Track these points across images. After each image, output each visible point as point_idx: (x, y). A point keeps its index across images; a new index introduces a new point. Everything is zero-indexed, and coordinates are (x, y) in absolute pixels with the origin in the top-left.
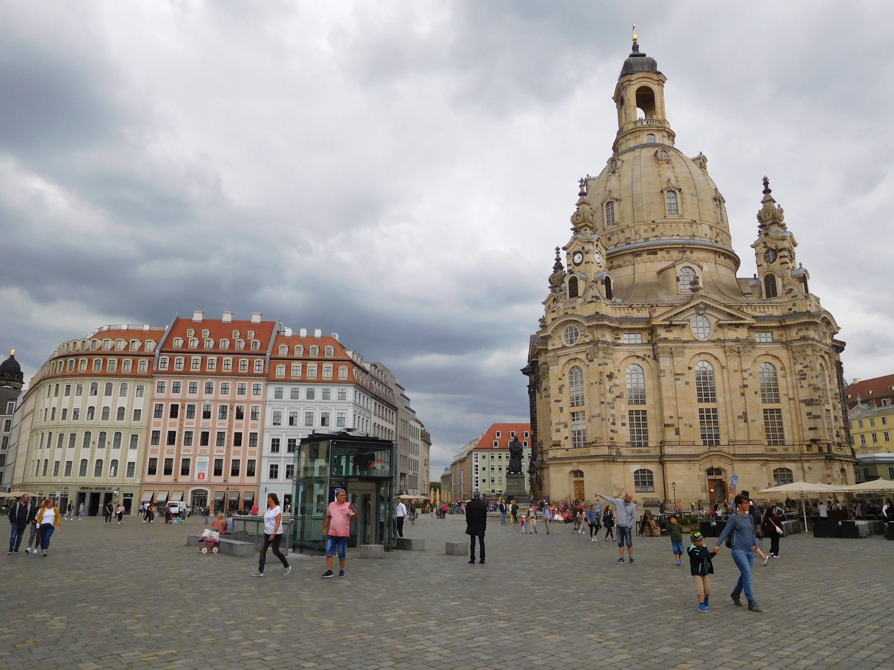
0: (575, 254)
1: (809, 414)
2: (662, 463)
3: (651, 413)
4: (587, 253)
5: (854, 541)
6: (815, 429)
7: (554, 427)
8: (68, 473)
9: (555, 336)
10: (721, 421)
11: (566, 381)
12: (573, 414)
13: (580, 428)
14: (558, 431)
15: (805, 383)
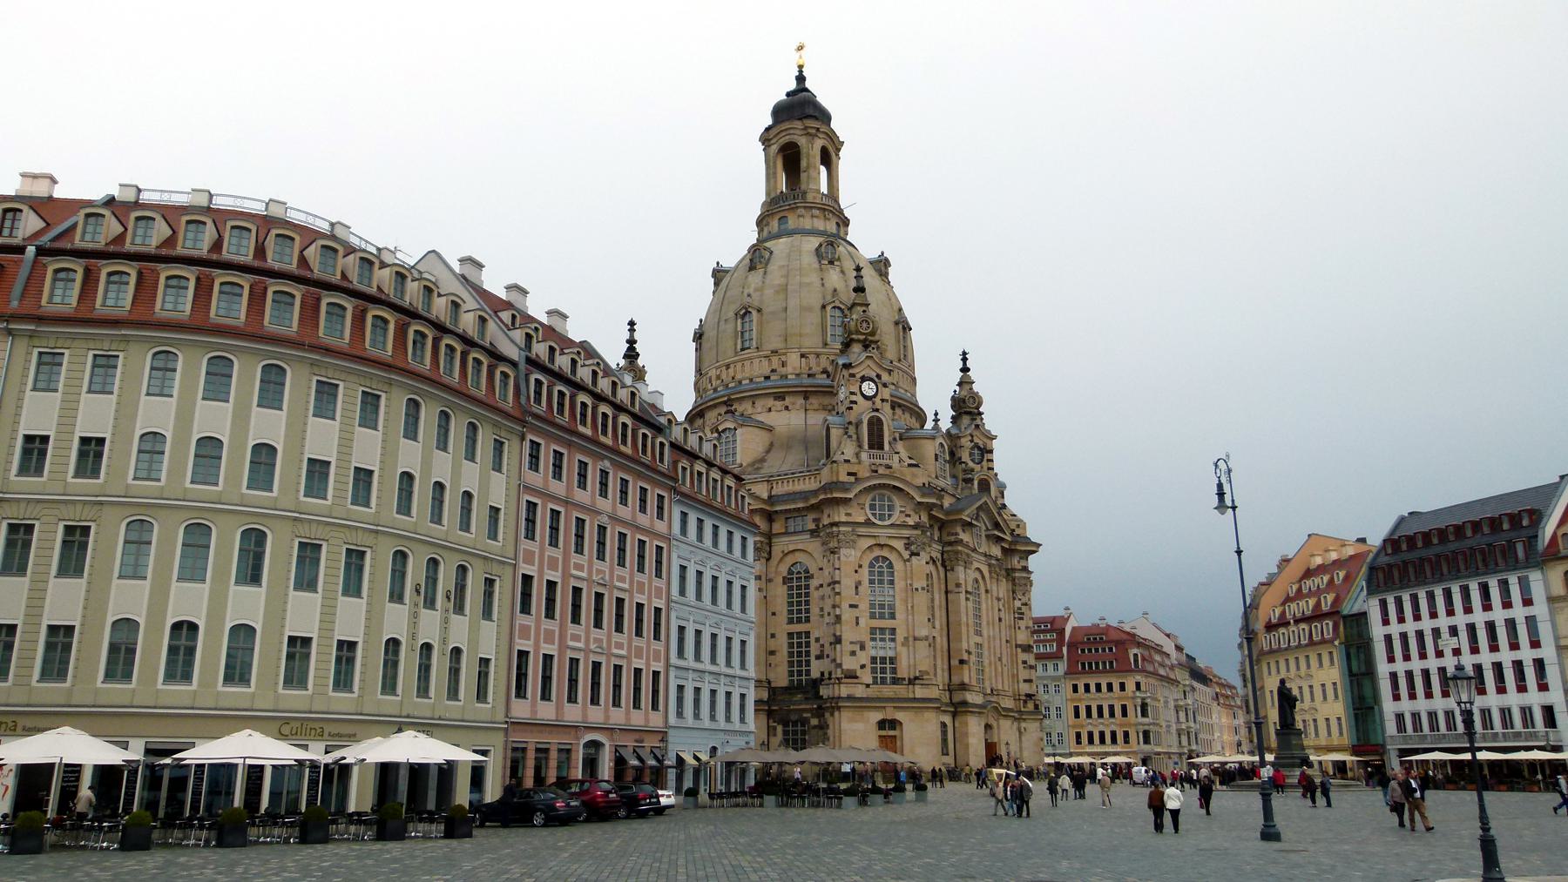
0: (863, 379)
1: (1025, 662)
2: (954, 715)
3: (938, 639)
4: (885, 385)
5: (529, 830)
6: (1030, 681)
7: (846, 646)
8: (343, 680)
9: (854, 503)
10: (986, 662)
11: (865, 574)
12: (873, 630)
13: (881, 653)
14: (853, 653)
15: (1022, 624)
